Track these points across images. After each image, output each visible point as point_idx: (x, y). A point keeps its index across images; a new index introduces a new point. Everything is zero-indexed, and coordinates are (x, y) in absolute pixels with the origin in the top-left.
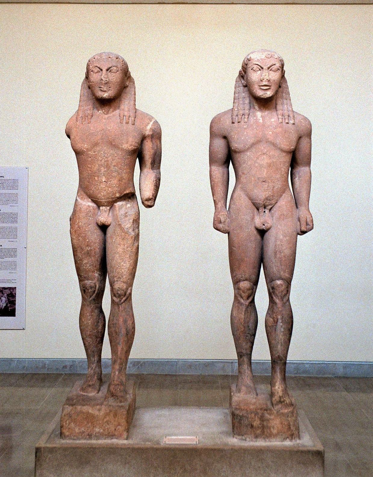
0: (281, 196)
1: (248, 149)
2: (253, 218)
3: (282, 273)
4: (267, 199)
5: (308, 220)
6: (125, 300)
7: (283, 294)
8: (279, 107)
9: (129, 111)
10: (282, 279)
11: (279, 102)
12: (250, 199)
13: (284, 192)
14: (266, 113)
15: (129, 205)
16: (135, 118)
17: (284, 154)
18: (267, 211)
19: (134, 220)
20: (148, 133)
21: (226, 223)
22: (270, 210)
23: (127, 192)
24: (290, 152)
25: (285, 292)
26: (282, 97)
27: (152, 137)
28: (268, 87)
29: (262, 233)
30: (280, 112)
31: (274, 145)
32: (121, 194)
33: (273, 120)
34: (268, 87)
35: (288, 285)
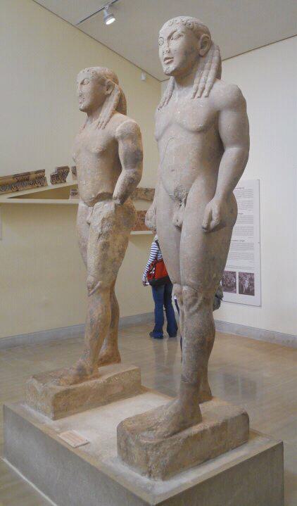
0: (190, 186)
1: (162, 135)
2: (171, 214)
3: (186, 277)
4: (177, 190)
5: (213, 214)
6: (94, 292)
7: (188, 303)
8: (196, 80)
9: (105, 117)
10: (187, 285)
11: (198, 74)
12: (167, 192)
13: (193, 181)
14: (185, 89)
15: (106, 205)
16: (108, 122)
17: (192, 135)
18: (183, 204)
19: (103, 219)
20: (117, 134)
21: (153, 220)
22: (185, 203)
23: (99, 192)
24: (200, 131)
25: (190, 301)
26: (203, 69)
27: (122, 137)
28: (170, 60)
29: (179, 228)
30: (195, 86)
31: (180, 125)
32: (95, 194)
33: (186, 97)
34: (170, 60)
35: (196, 293)
